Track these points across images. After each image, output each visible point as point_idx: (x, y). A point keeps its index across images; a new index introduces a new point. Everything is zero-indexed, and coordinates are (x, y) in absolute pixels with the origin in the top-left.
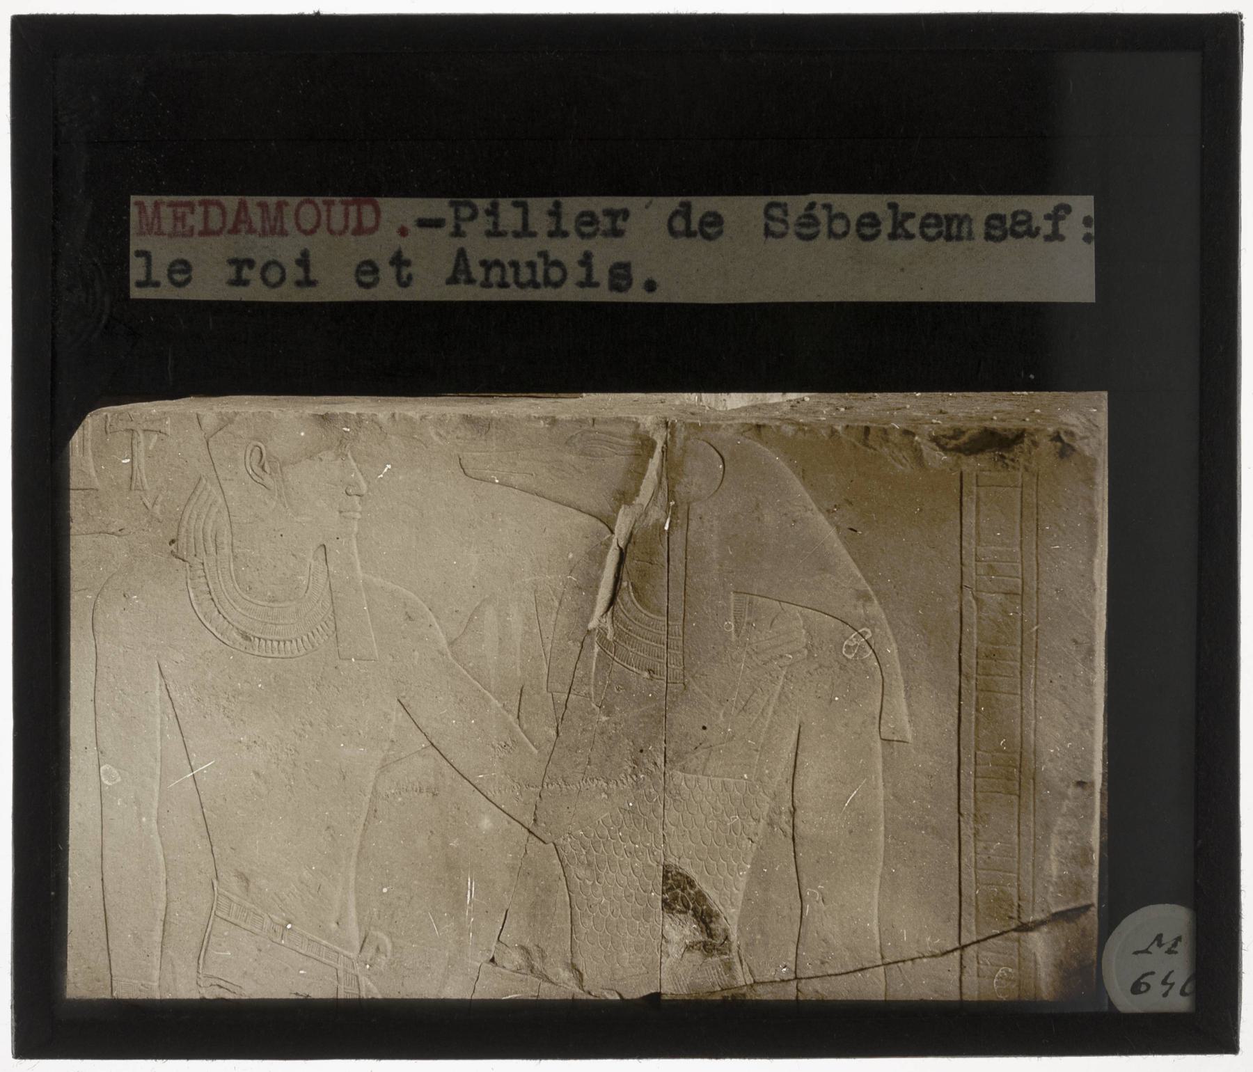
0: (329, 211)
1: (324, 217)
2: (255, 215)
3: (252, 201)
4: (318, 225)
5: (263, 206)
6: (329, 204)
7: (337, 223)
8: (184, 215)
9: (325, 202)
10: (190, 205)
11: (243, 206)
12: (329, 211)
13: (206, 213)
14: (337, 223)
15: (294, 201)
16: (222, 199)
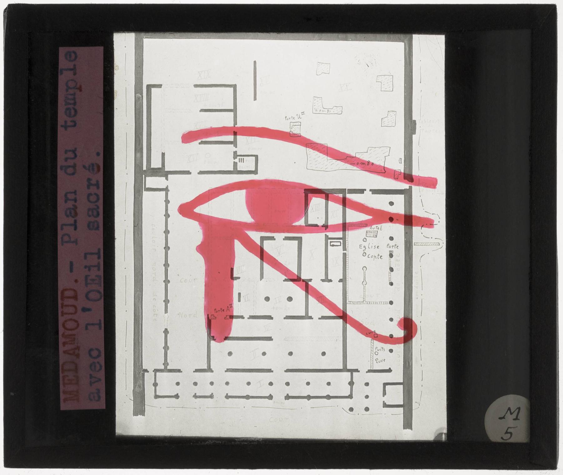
0: (66, 314)
1: (70, 317)
2: (68, 347)
3: (61, 349)
4: (71, 320)
5: (64, 344)
6: (63, 314)
7: (72, 310)
8: (69, 380)
9: (62, 315)
10: (64, 377)
11: (65, 352)
12: (66, 314)
13: (69, 370)
14: (72, 310)
15: (61, 330)
16: (61, 362)
